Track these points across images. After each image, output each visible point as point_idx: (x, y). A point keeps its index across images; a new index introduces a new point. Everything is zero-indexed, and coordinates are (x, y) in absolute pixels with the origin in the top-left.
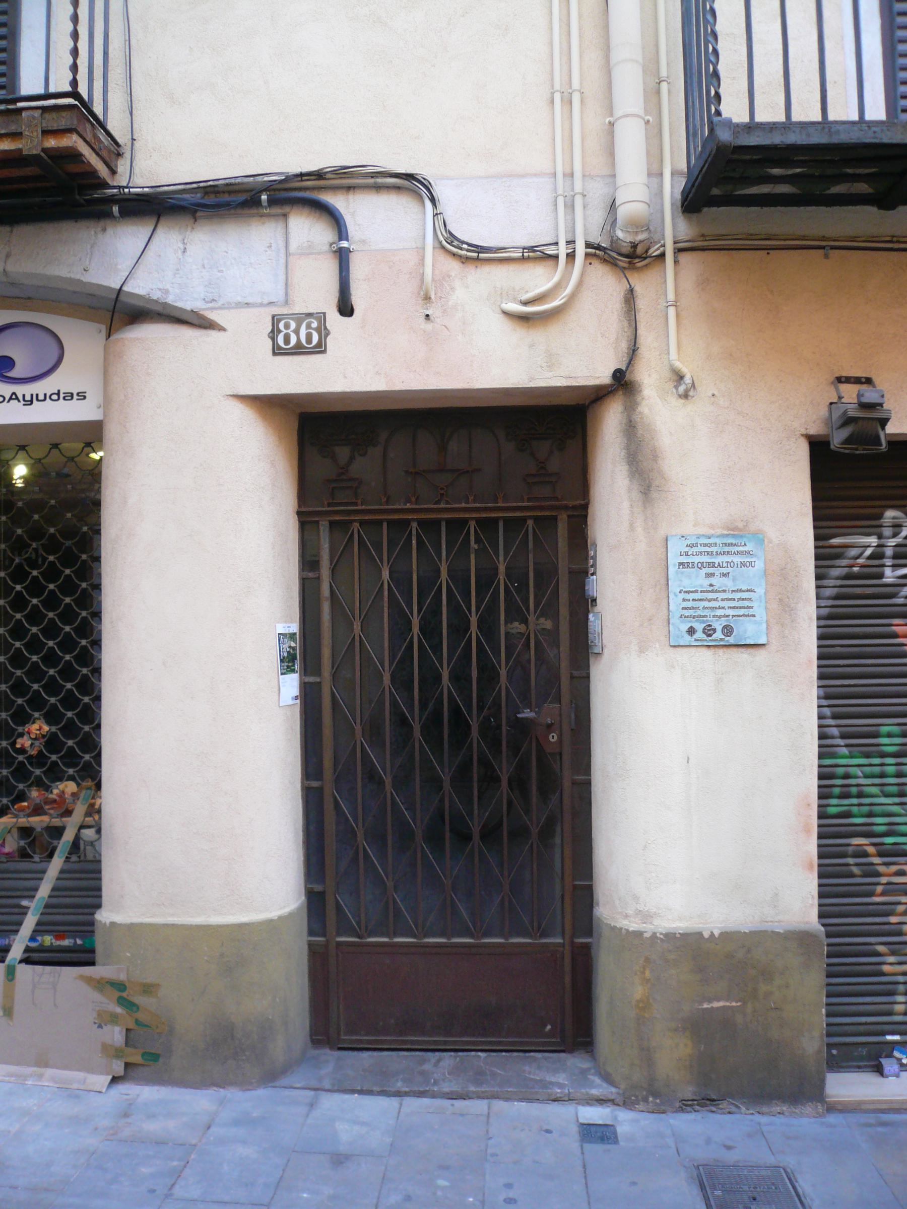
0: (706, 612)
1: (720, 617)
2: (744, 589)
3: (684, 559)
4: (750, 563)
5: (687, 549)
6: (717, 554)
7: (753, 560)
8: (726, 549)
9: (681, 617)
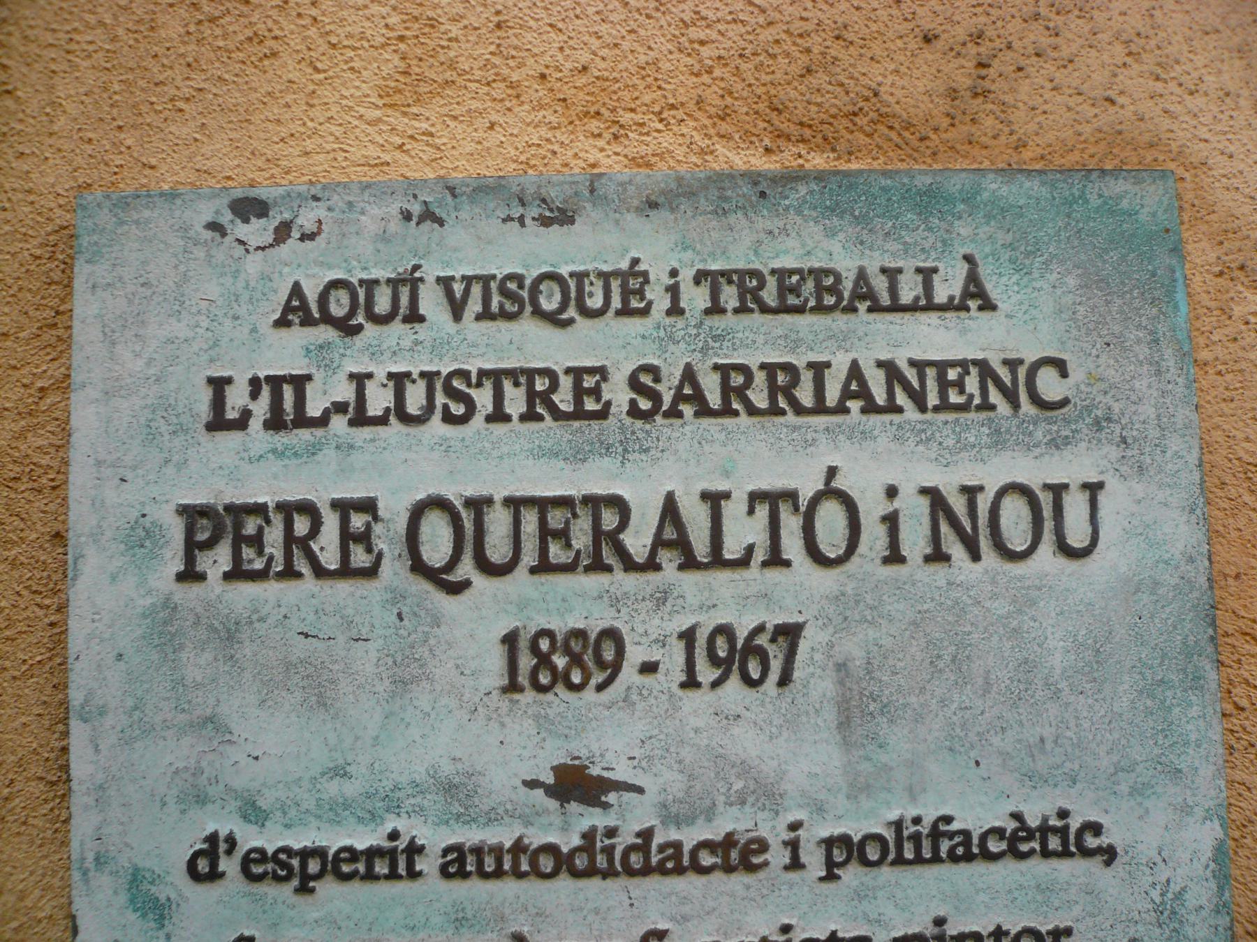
2: (977, 814)
3: (254, 471)
4: (1045, 505)
5: (287, 352)
6: (654, 400)
7: (1072, 467)
8: (758, 342)
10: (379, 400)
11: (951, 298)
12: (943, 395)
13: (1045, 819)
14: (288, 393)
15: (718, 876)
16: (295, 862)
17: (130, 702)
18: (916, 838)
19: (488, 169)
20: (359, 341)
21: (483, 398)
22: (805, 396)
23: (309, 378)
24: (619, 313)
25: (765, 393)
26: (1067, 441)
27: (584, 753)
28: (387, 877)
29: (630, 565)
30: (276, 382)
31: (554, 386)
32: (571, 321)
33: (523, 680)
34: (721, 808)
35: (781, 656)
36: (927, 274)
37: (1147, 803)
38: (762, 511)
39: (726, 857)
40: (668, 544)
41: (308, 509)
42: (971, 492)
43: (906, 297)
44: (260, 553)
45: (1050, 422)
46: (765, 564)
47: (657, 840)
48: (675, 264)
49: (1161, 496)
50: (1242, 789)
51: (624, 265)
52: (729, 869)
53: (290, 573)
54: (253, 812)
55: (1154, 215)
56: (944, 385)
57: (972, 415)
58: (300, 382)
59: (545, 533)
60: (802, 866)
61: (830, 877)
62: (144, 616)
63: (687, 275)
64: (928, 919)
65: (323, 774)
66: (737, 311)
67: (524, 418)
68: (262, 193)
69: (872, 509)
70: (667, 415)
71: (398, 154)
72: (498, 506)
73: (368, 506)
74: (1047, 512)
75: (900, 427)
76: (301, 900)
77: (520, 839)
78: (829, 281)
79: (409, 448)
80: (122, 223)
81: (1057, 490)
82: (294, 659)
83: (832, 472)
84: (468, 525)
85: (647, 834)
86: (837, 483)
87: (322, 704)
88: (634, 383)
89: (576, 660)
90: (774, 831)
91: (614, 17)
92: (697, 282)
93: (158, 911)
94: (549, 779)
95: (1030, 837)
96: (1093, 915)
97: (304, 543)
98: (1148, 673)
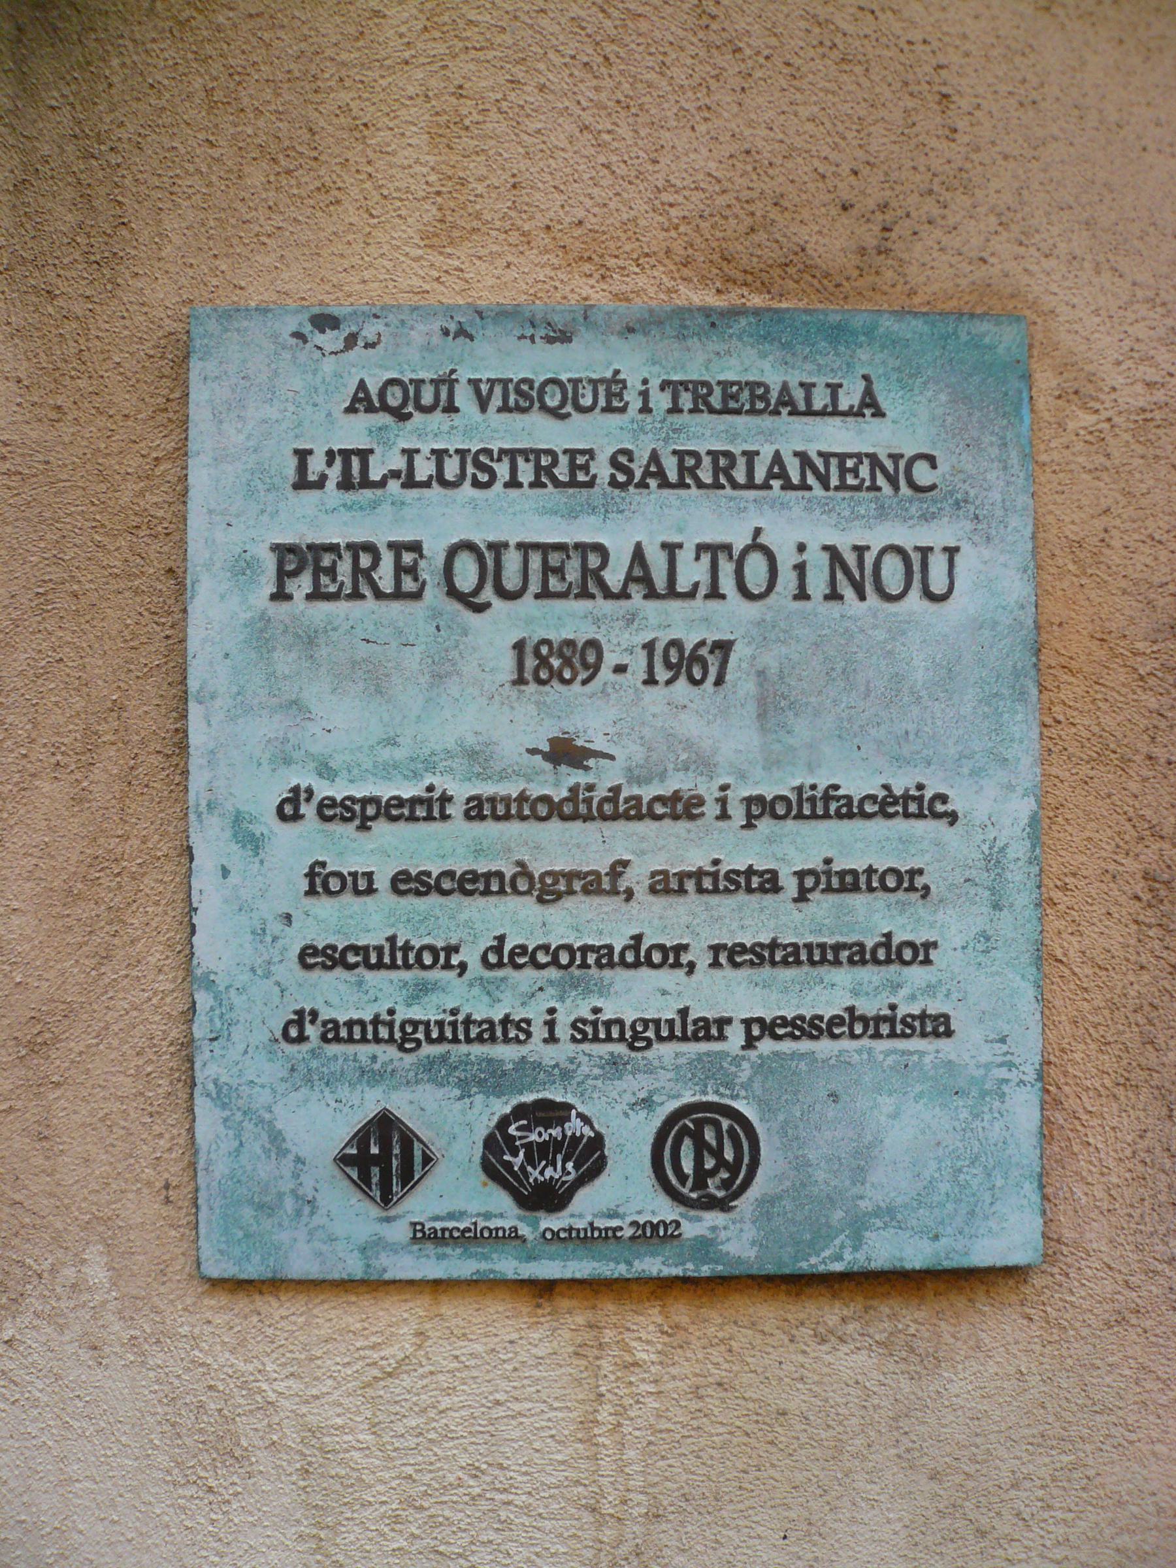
0: (521, 995)
1: (639, 1036)
2: (858, 784)
3: (328, 520)
4: (915, 562)
5: (355, 432)
7: (937, 535)
8: (706, 434)
9: (296, 1028)
10: (424, 469)
11: (852, 407)
12: (842, 478)
13: (907, 790)
14: (355, 462)
15: (667, 822)
16: (357, 807)
17: (235, 689)
18: (812, 799)
19: (506, 298)
20: (409, 425)
21: (502, 470)
22: (740, 476)
23: (371, 451)
24: (604, 410)
25: (710, 473)
26: (934, 516)
27: (571, 729)
28: (425, 819)
29: (608, 594)
30: (346, 454)
31: (555, 462)
32: (568, 415)
33: (528, 675)
34: (670, 773)
35: (717, 664)
36: (834, 388)
37: (982, 782)
38: (706, 558)
39: (674, 808)
40: (637, 580)
41: (370, 548)
42: (860, 550)
43: (818, 405)
44: (334, 580)
45: (921, 501)
46: (707, 597)
47: (624, 794)
48: (646, 375)
49: (1002, 559)
50: (1056, 781)
51: (609, 374)
52: (676, 817)
53: (356, 595)
54: (326, 771)
55: (1009, 349)
56: (843, 471)
57: (863, 494)
58: (364, 455)
59: (547, 569)
60: (729, 817)
61: (749, 826)
62: (246, 626)
63: (654, 384)
64: (820, 860)
65: (379, 743)
66: (691, 411)
67: (532, 485)
68: (336, 311)
69: (786, 559)
70: (637, 486)
71: (435, 285)
72: (512, 549)
73: (415, 547)
74: (916, 567)
75: (809, 501)
76: (362, 836)
77: (524, 791)
78: (761, 391)
79: (447, 505)
80: (227, 330)
81: (925, 551)
82: (358, 658)
83: (758, 532)
84: (490, 563)
85: (616, 790)
86: (762, 540)
87: (379, 691)
88: (614, 462)
89: (567, 662)
90: (708, 790)
91: (604, 183)
92: (662, 389)
93: (253, 843)
94: (547, 749)
95: (895, 803)
96: (939, 861)
97: (367, 574)
98: (986, 688)
